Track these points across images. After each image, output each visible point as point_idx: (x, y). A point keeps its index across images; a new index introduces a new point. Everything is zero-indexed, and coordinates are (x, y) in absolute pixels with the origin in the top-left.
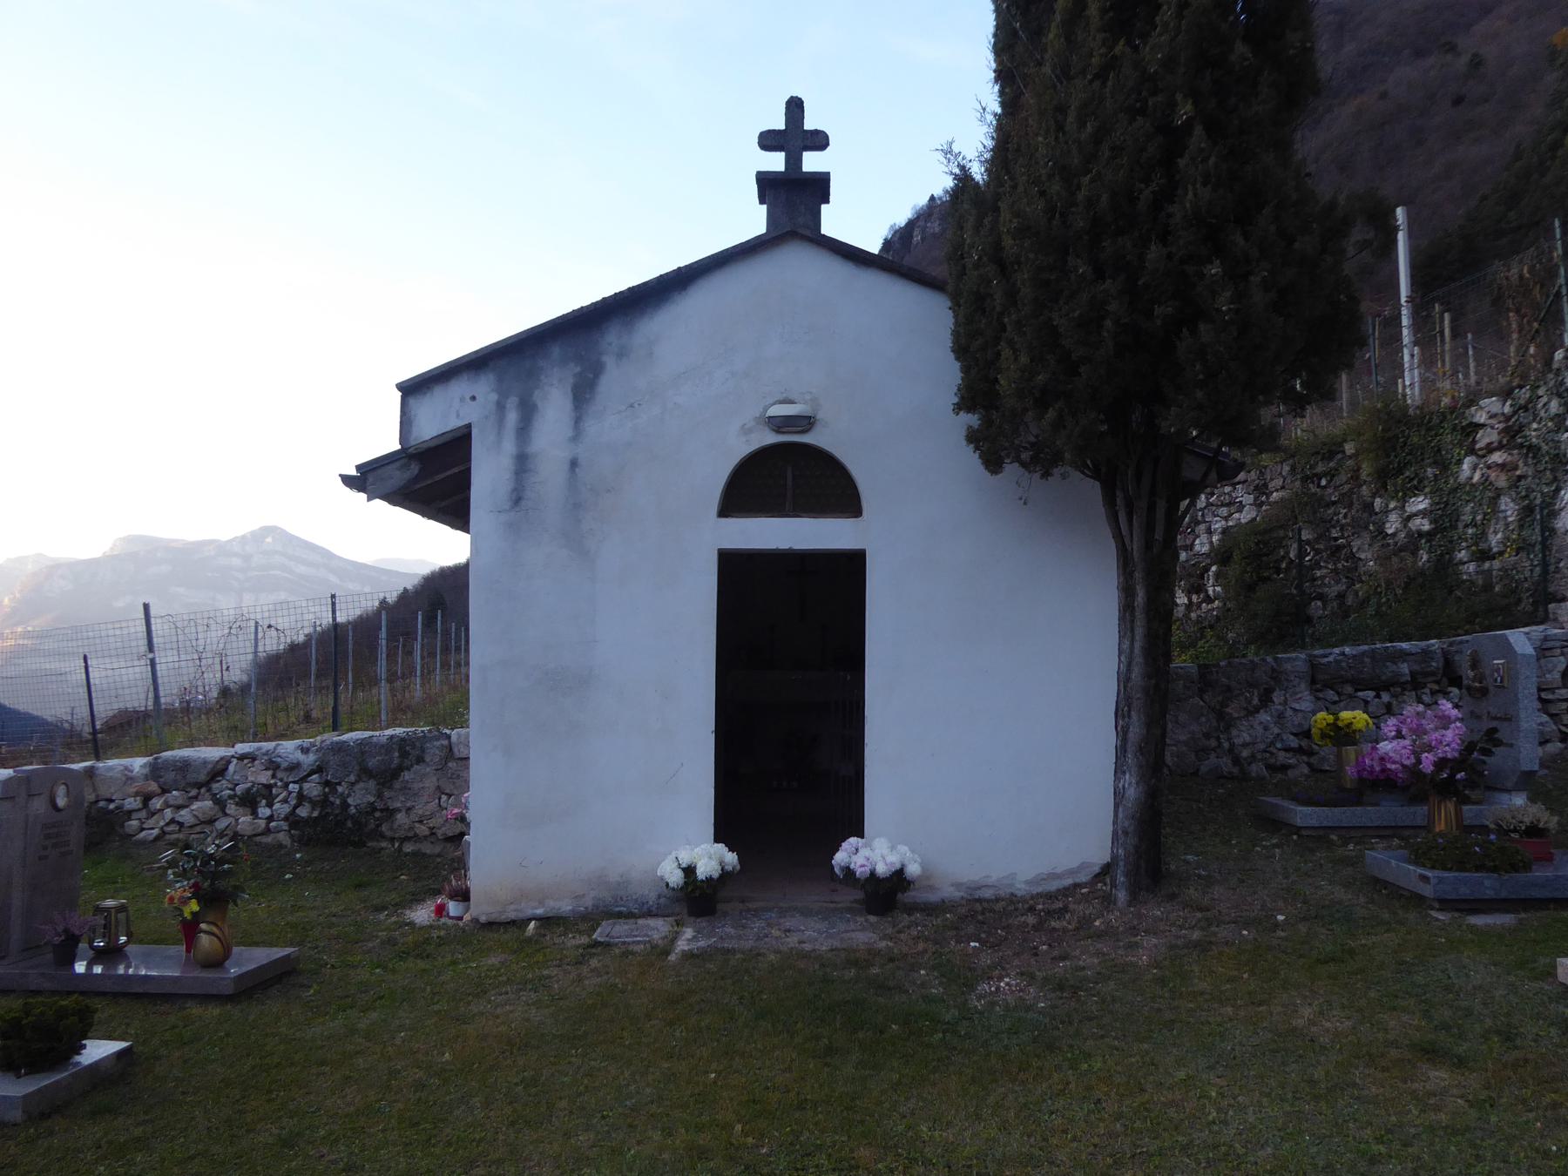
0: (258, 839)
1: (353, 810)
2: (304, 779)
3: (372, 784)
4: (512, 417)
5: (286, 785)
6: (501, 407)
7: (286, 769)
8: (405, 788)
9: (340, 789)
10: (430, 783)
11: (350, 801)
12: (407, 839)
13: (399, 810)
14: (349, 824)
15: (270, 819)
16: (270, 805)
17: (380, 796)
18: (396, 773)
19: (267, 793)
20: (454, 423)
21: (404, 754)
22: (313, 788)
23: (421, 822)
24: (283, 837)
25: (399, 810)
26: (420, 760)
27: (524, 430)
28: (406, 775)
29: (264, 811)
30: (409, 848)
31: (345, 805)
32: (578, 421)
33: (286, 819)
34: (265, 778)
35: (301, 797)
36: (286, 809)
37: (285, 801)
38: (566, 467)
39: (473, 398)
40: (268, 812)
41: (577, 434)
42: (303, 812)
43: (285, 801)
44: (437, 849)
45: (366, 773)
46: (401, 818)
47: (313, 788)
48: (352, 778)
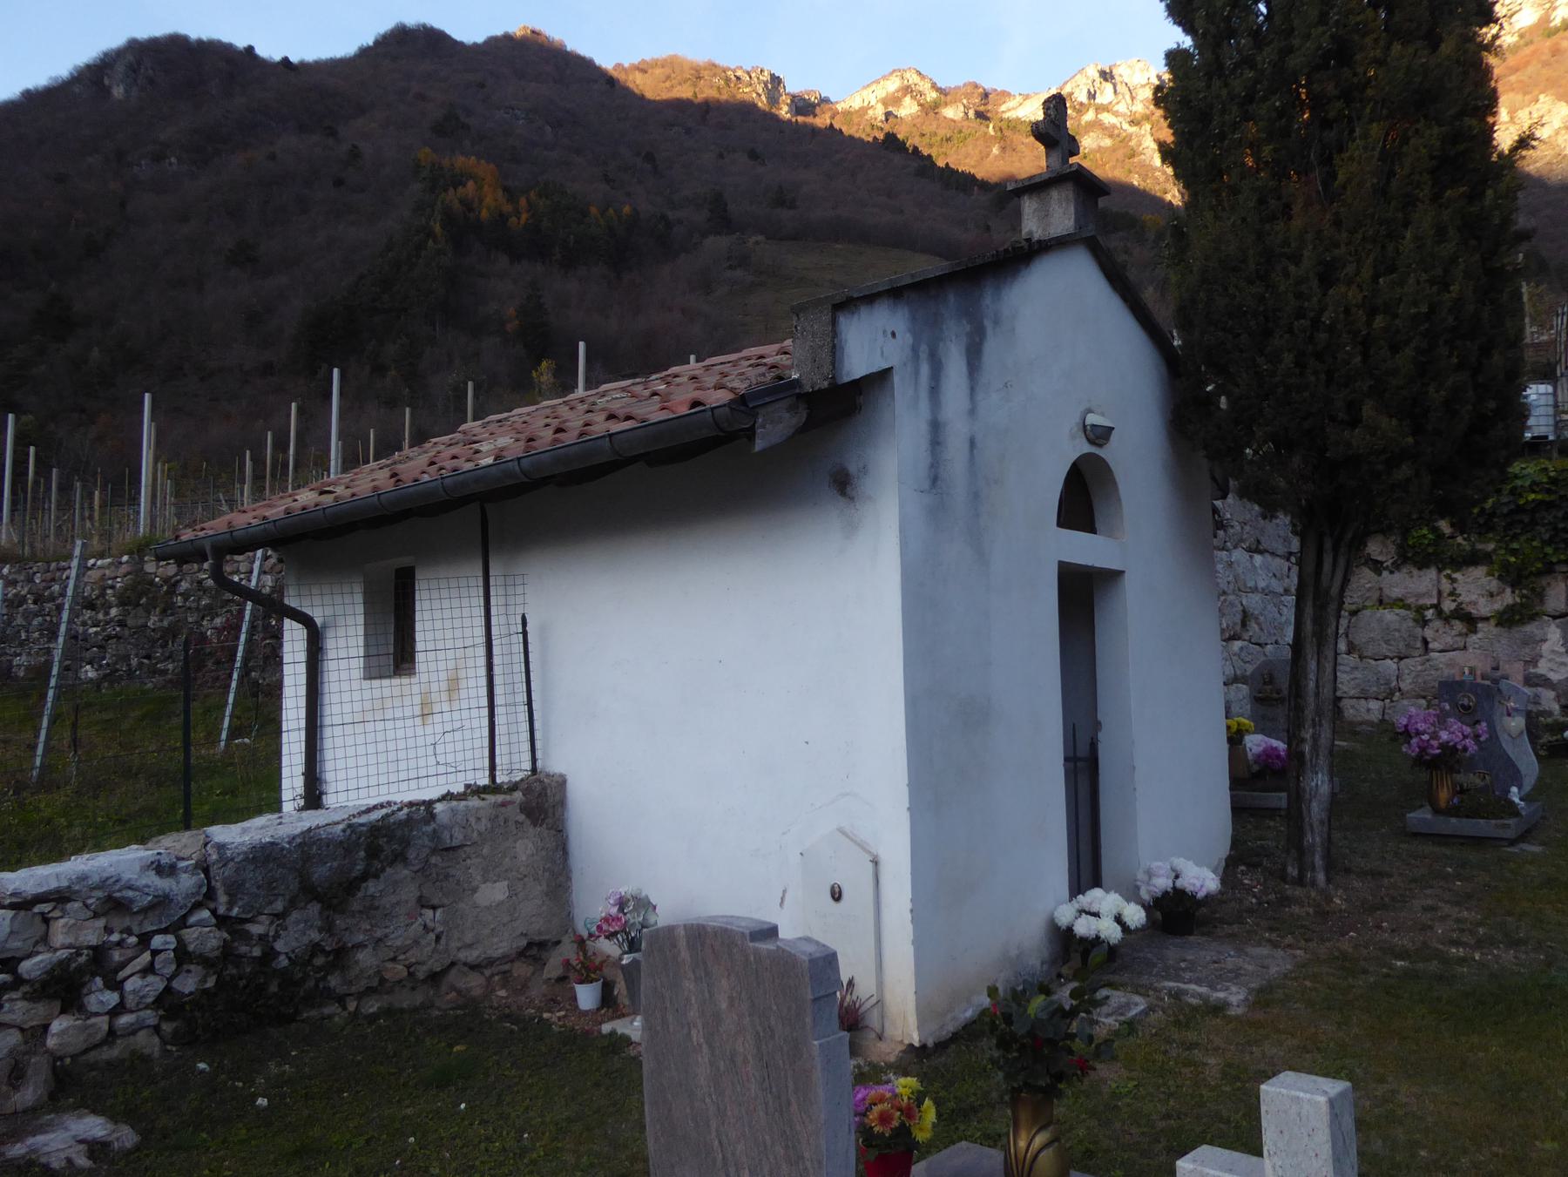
0: (92, 1056)
1: (283, 962)
2: (183, 923)
3: (314, 909)
4: (925, 369)
5: (145, 939)
6: (915, 350)
7: (145, 910)
8: (371, 909)
9: (256, 929)
10: (409, 893)
11: (279, 946)
12: (370, 991)
13: (361, 946)
14: (274, 988)
15: (115, 1012)
16: (116, 985)
17: (328, 928)
18: (352, 886)
19: (99, 962)
20: (879, 365)
21: (373, 852)
22: (203, 935)
23: (394, 959)
24: (147, 1043)
25: (361, 946)
26: (400, 858)
27: (935, 390)
28: (372, 887)
29: (101, 998)
30: (372, 1006)
31: (270, 954)
32: (972, 390)
33: (159, 1002)
34: (91, 935)
35: (183, 955)
36: (155, 984)
37: (149, 970)
38: (966, 446)
39: (893, 334)
40: (112, 998)
41: (972, 412)
42: (188, 984)
43: (149, 970)
44: (418, 998)
45: (309, 891)
46: (365, 958)
47: (203, 935)
48: (279, 906)
